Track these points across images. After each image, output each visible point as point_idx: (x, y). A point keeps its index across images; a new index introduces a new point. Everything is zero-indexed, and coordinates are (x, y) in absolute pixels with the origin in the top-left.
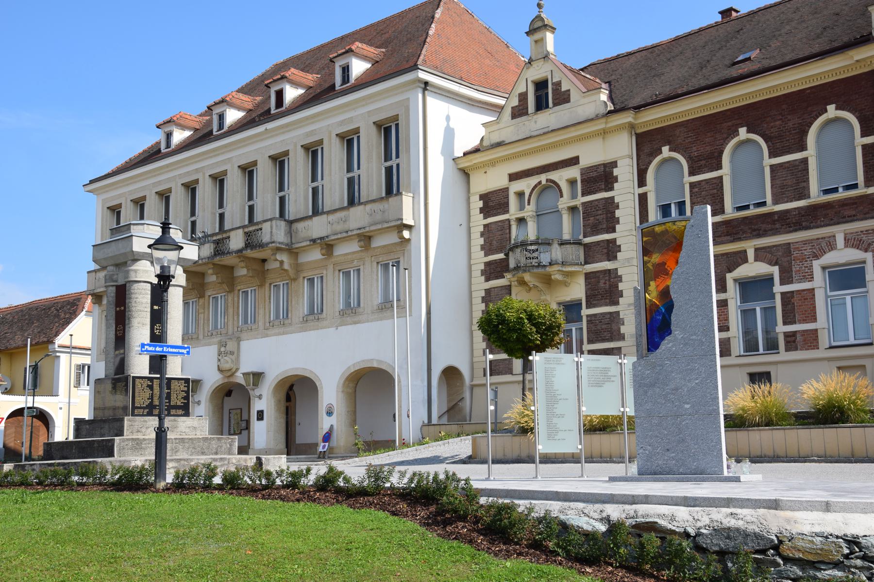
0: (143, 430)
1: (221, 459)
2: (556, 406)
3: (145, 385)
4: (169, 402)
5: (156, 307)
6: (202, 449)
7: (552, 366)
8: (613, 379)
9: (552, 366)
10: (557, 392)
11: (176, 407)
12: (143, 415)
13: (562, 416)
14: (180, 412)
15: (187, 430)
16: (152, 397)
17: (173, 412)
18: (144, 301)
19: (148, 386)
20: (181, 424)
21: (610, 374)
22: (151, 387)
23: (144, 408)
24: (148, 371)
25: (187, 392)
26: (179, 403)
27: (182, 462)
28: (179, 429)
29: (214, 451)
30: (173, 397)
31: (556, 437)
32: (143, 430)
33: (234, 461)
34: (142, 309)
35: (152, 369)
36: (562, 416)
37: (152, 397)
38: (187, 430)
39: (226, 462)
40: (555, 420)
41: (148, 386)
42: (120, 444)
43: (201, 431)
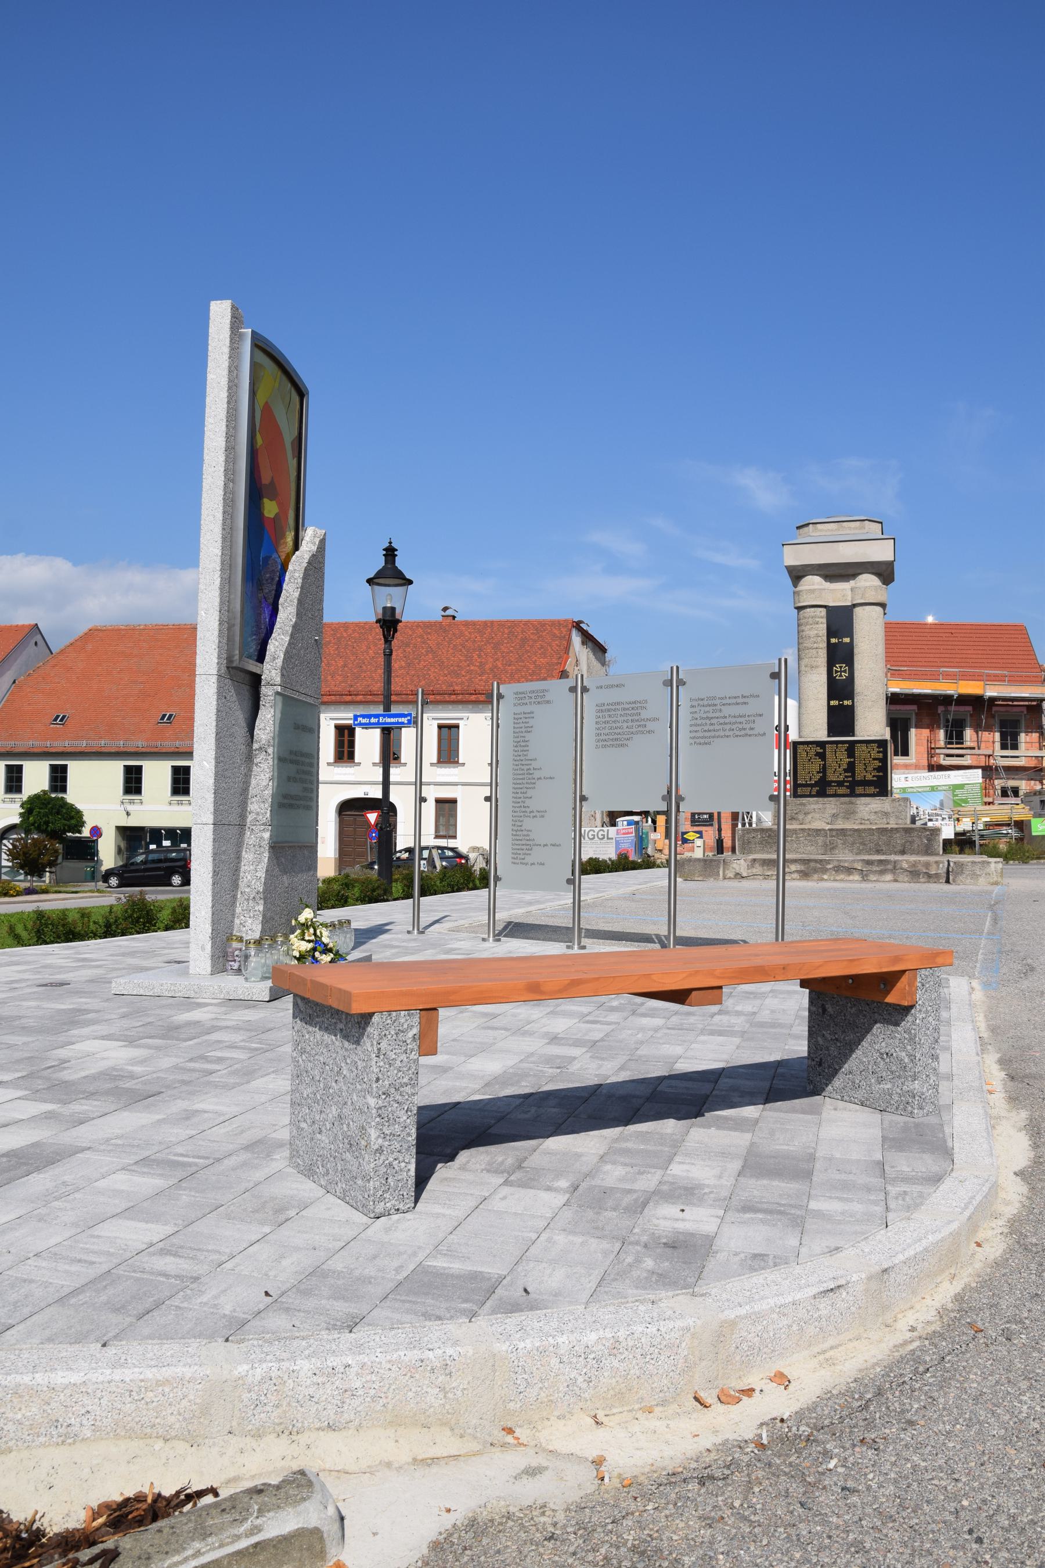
0: (801, 817)
1: (881, 862)
2: (530, 793)
3: (812, 753)
4: (853, 775)
5: (833, 640)
6: (877, 844)
7: (527, 709)
8: (650, 726)
9: (527, 709)
10: (534, 764)
11: (865, 783)
12: (810, 796)
13: (542, 814)
14: (871, 790)
15: (873, 817)
16: (824, 770)
17: (859, 790)
18: (812, 633)
19: (817, 754)
20: (862, 808)
21: (645, 714)
22: (822, 756)
23: (812, 786)
24: (826, 732)
25: (884, 761)
26: (869, 777)
27: (812, 864)
28: (859, 815)
29: (899, 848)
30: (859, 768)
31: (529, 859)
32: (801, 817)
33: (905, 865)
34: (809, 645)
35: (832, 730)
36: (542, 814)
37: (824, 770)
38: (873, 817)
39: (890, 867)
40: (528, 823)
41: (817, 754)
42: (743, 835)
43: (897, 817)
